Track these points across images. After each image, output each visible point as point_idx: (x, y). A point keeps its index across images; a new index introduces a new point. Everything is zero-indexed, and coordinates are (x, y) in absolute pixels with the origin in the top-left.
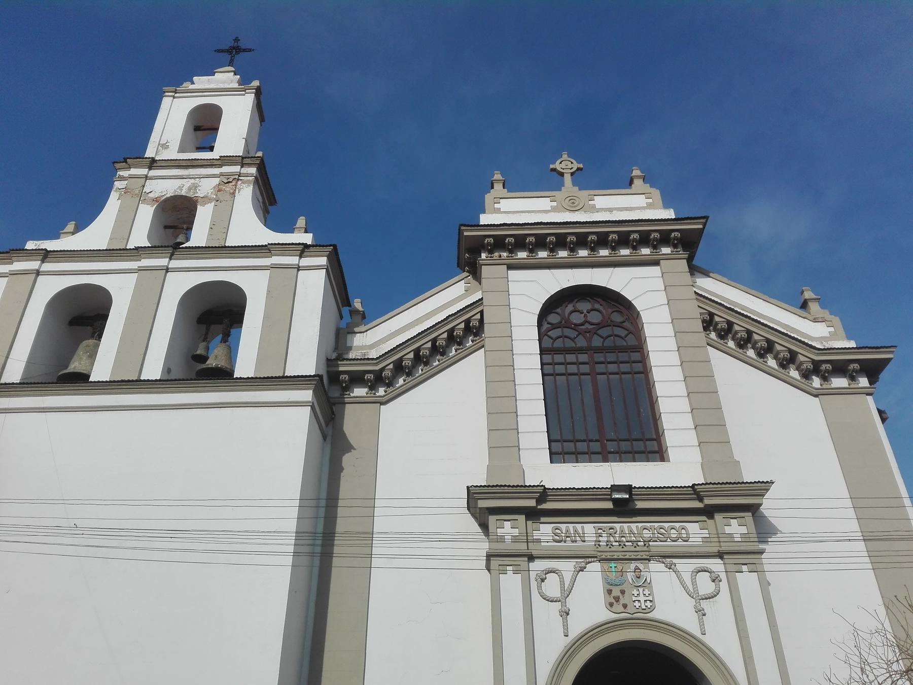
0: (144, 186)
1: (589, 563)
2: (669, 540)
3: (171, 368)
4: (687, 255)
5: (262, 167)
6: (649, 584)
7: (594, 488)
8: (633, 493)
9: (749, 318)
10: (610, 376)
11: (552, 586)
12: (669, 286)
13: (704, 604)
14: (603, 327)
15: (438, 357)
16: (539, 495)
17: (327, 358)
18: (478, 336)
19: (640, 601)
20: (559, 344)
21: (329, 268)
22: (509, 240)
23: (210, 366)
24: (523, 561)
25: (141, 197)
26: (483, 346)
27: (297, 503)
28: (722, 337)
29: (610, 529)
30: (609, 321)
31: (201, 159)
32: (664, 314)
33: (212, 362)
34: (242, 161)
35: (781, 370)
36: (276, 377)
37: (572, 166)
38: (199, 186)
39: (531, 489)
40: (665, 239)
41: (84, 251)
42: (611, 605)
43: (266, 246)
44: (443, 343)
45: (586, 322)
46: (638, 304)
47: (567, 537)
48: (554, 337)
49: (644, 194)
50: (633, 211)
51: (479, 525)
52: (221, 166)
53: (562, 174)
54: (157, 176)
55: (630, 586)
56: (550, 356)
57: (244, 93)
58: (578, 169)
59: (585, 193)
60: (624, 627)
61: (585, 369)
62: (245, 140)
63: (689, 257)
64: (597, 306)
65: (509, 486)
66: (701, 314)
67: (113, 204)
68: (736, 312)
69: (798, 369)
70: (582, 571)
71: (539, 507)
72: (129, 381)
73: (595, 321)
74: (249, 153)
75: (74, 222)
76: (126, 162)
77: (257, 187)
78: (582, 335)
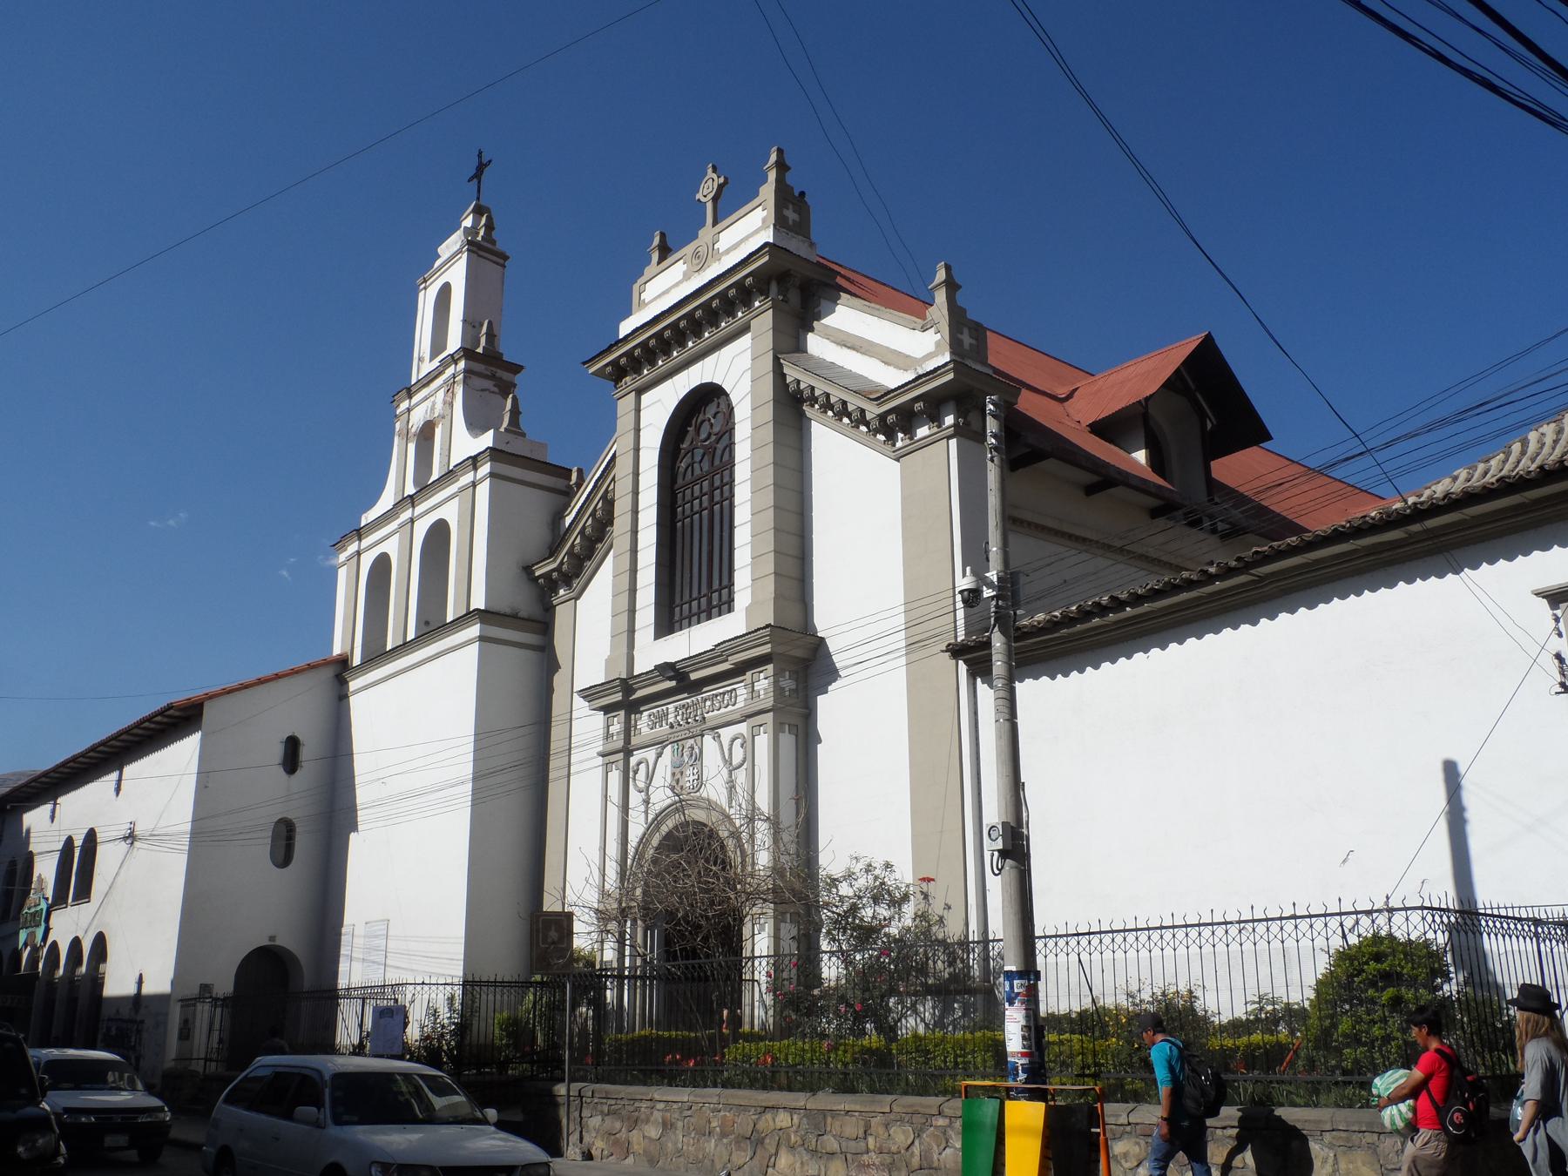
0: (408, 422)
17: (523, 568)
24: (621, 755)
27: (472, 739)
45: (709, 435)
46: (734, 399)
58: (721, 187)
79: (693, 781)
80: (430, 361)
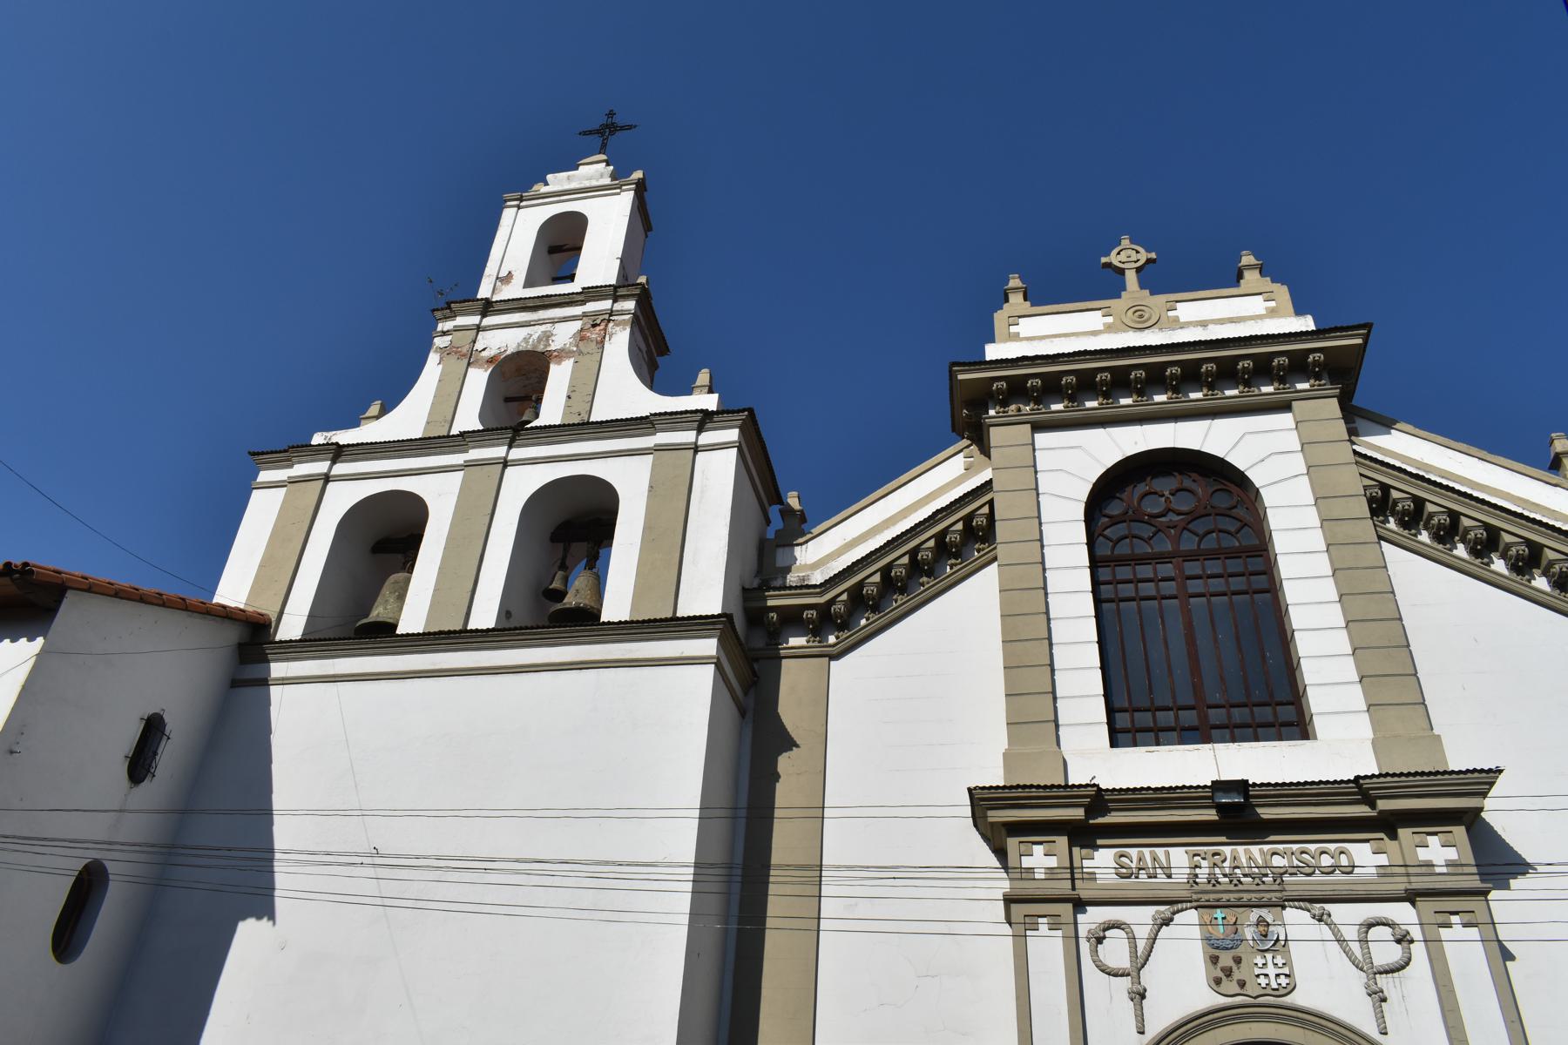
0: (475, 342)
1: (1179, 911)
2: (1317, 872)
3: (511, 610)
4: (1338, 391)
5: (644, 300)
6: (1284, 946)
7: (1184, 787)
8: (1251, 793)
9: (1452, 490)
10: (1213, 598)
11: (1116, 951)
12: (1307, 443)
13: (1382, 981)
14: (1198, 518)
15: (925, 579)
16: (1089, 800)
17: (744, 590)
18: (988, 542)
19: (1266, 975)
20: (1123, 549)
21: (744, 446)
22: (1032, 383)
23: (568, 606)
25: (470, 357)
26: (995, 559)
27: (697, 813)
28: (1403, 524)
29: (1215, 854)
30: (1209, 507)
31: (556, 295)
32: (1303, 491)
33: (571, 600)
34: (614, 293)
35: (1514, 576)
36: (661, 620)
37: (1139, 256)
38: (552, 334)
39: (1075, 792)
40: (1299, 366)
41: (389, 442)
42: (1218, 981)
43: (647, 417)
44: (928, 556)
45: (1169, 510)
46: (1256, 477)
47: (1140, 869)
48: (1114, 538)
49: (1260, 294)
50: (1242, 323)
51: (993, 852)
52: (583, 303)
53: (1121, 272)
54: (493, 326)
55: (1249, 949)
56: (1109, 569)
57: (618, 191)
58: (1149, 261)
59: (1162, 299)
60: (1240, 1018)
61: (1169, 588)
62: (619, 261)
63: (1341, 393)
64: (1187, 483)
65: (1038, 787)
66: (1366, 488)
67: (432, 370)
68: (1429, 481)
69: (1545, 574)
70: (1167, 925)
71: (1091, 822)
72: (450, 632)
73: (1185, 508)
74: (627, 280)
75: (379, 402)
76: (449, 308)
77: (636, 329)
78: (1163, 532)
79: (1278, 975)
80: (524, 287)
